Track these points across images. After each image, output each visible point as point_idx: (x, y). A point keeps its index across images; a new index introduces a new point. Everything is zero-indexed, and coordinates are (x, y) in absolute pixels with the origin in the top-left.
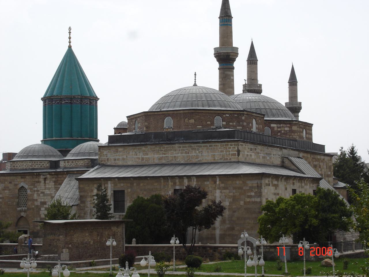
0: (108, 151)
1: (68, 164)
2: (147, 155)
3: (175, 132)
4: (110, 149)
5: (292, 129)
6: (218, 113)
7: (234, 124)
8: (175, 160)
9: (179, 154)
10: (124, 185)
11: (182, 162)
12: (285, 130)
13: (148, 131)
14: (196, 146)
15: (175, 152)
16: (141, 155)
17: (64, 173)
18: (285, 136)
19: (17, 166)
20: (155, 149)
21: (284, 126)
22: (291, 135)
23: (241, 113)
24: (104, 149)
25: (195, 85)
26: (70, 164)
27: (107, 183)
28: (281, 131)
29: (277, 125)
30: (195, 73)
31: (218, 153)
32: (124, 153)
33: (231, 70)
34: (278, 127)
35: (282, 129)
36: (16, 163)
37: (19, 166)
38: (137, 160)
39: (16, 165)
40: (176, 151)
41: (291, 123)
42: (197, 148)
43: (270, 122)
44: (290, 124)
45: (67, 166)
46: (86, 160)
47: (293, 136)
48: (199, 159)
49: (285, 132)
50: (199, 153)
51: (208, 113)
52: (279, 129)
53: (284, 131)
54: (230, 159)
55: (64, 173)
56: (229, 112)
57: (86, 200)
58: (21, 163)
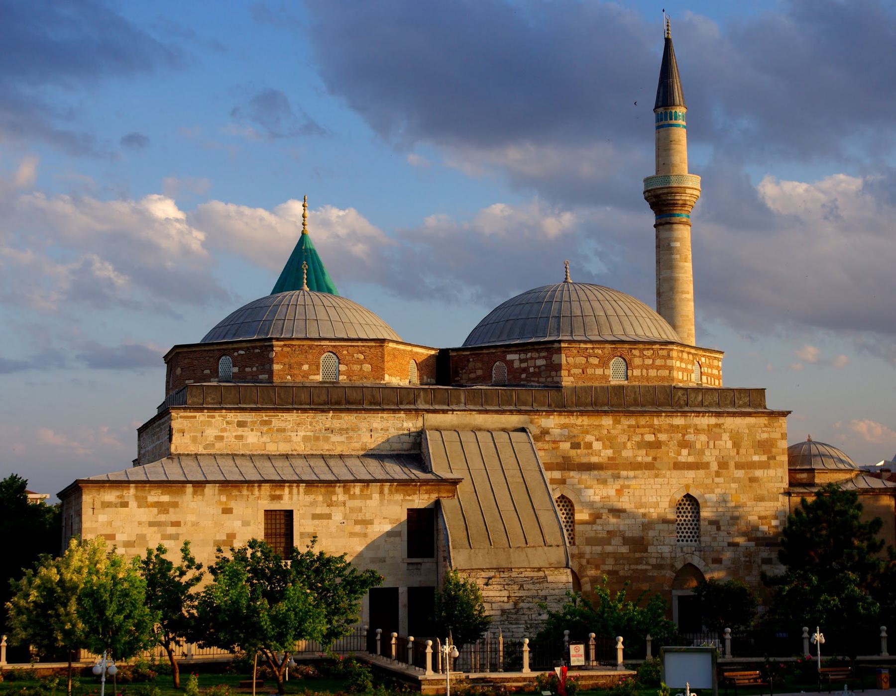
5: (551, 363)
6: (224, 349)
7: (255, 369)
12: (537, 365)
18: (536, 379)
21: (535, 356)
22: (550, 376)
23: (266, 344)
28: (528, 367)
29: (520, 354)
33: (668, 226)
34: (521, 361)
35: (531, 363)
41: (550, 348)
43: (503, 349)
44: (547, 350)
47: (553, 377)
49: (537, 370)
51: (205, 351)
52: (524, 365)
53: (535, 367)
56: (244, 345)
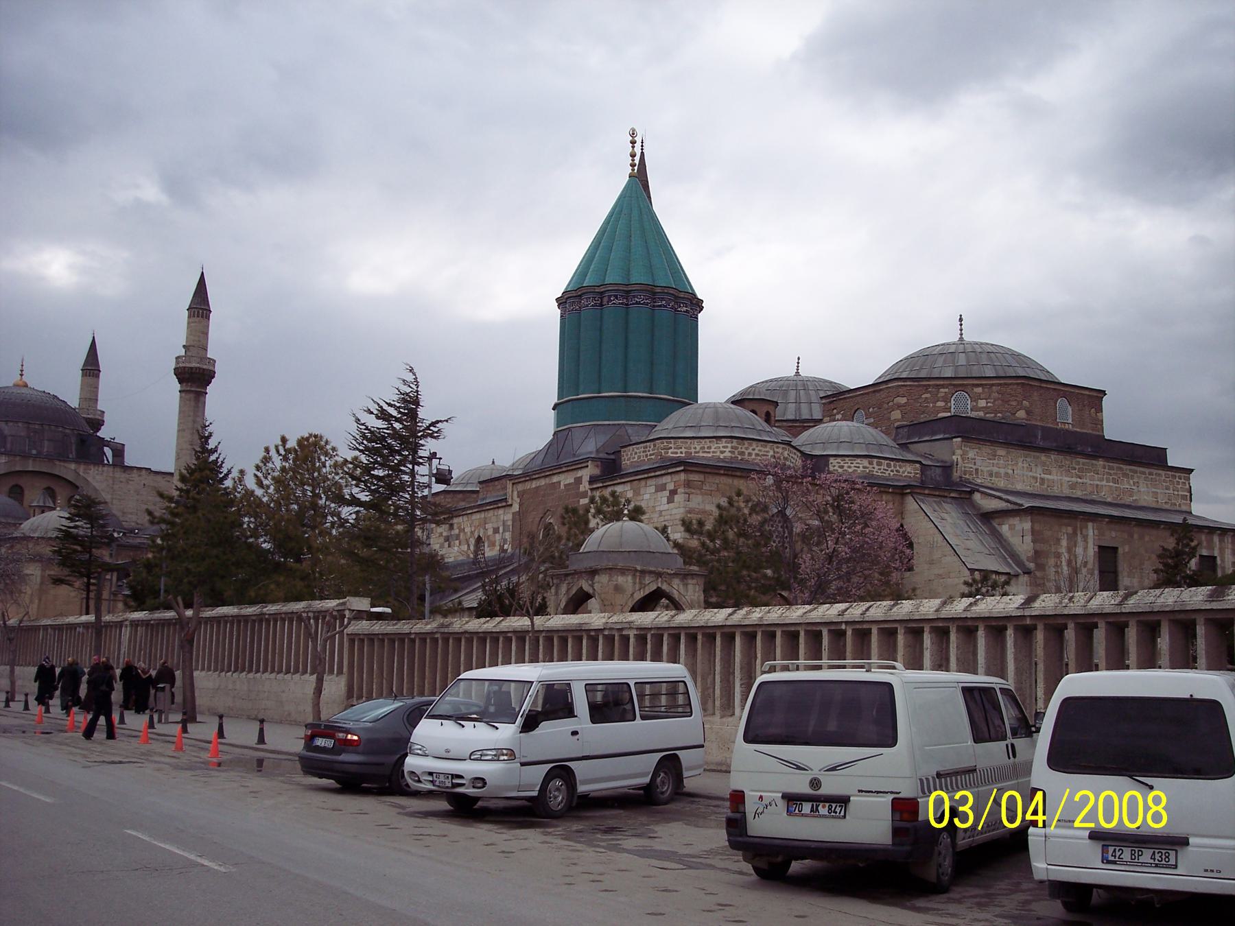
0: (977, 450)
1: (880, 469)
2: (1050, 474)
3: (1076, 431)
4: (979, 449)
8: (1097, 492)
9: (1103, 480)
10: (1116, 536)
11: (1109, 500)
13: (1030, 420)
14: (1130, 470)
15: (1096, 476)
16: (1038, 472)
17: (887, 490)
19: (750, 454)
20: (1063, 464)
24: (969, 444)
25: (961, 339)
26: (884, 469)
27: (1087, 527)
30: (961, 316)
31: (1162, 491)
32: (1007, 462)
36: (746, 445)
37: (757, 455)
38: (1033, 481)
39: (747, 449)
40: (1098, 474)
42: (1130, 474)
45: (877, 472)
46: (918, 465)
48: (1134, 498)
50: (1134, 484)
54: (1180, 505)
55: (887, 490)
57: (1047, 562)
58: (762, 446)
